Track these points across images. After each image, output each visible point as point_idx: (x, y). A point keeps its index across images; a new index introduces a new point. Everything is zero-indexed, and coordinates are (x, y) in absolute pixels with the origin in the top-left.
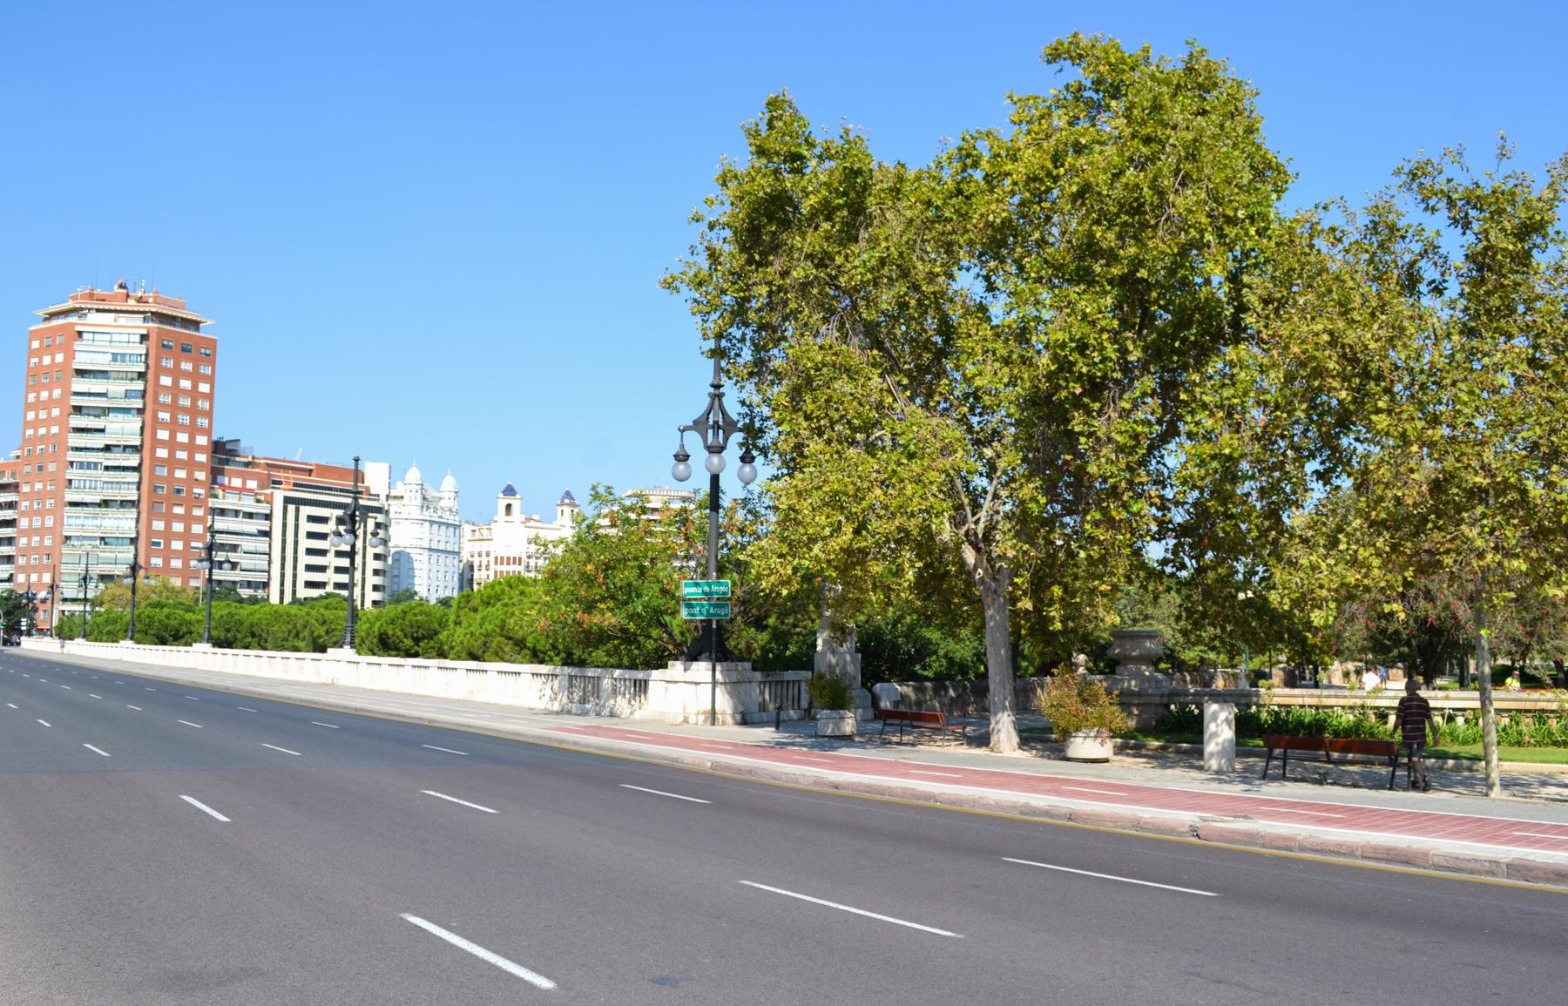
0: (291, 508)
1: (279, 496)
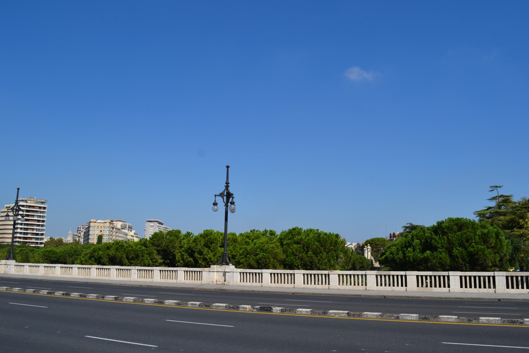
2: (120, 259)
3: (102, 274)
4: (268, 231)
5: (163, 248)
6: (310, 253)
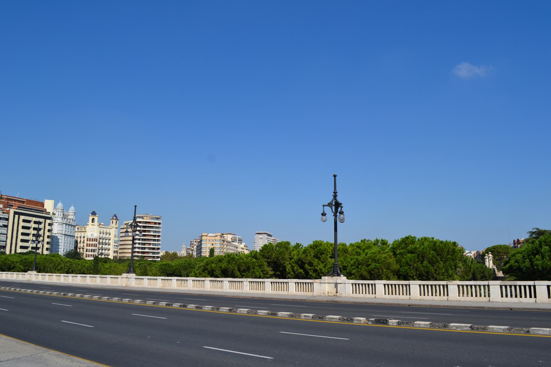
0: (17, 216)
1: (12, 211)
2: (232, 272)
3: (215, 286)
4: (379, 240)
5: (273, 260)
6: (425, 263)
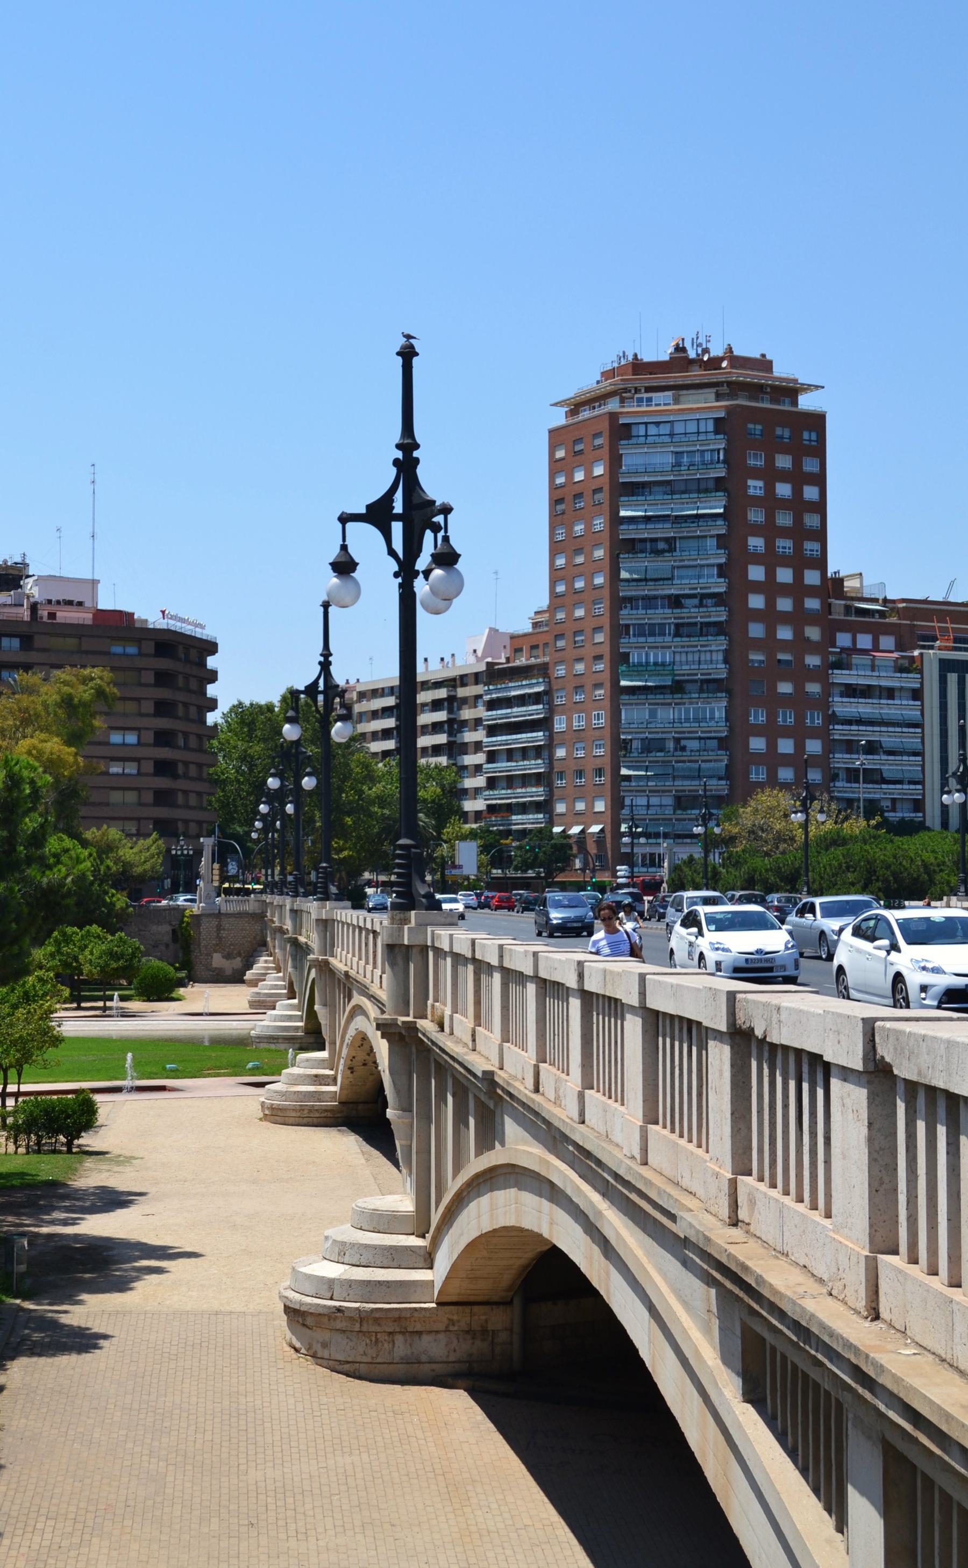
0: (952, 678)
